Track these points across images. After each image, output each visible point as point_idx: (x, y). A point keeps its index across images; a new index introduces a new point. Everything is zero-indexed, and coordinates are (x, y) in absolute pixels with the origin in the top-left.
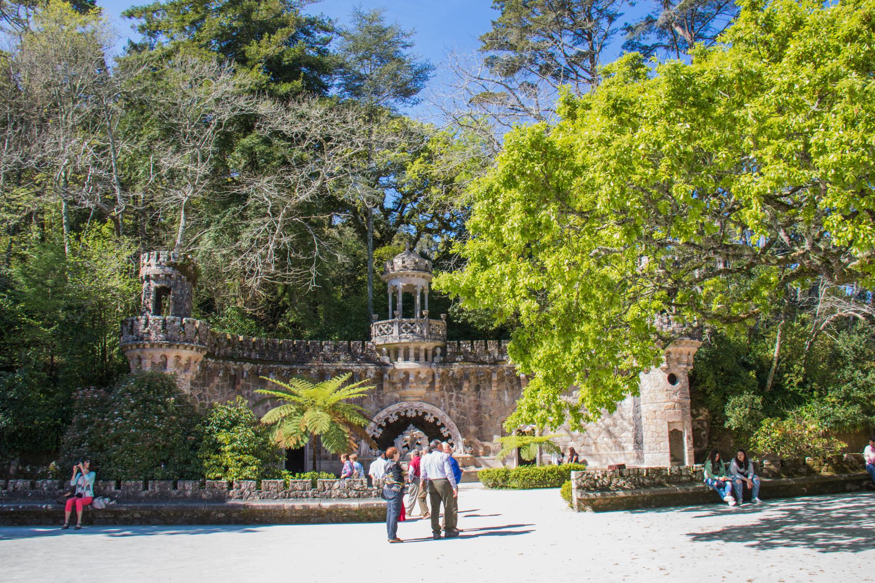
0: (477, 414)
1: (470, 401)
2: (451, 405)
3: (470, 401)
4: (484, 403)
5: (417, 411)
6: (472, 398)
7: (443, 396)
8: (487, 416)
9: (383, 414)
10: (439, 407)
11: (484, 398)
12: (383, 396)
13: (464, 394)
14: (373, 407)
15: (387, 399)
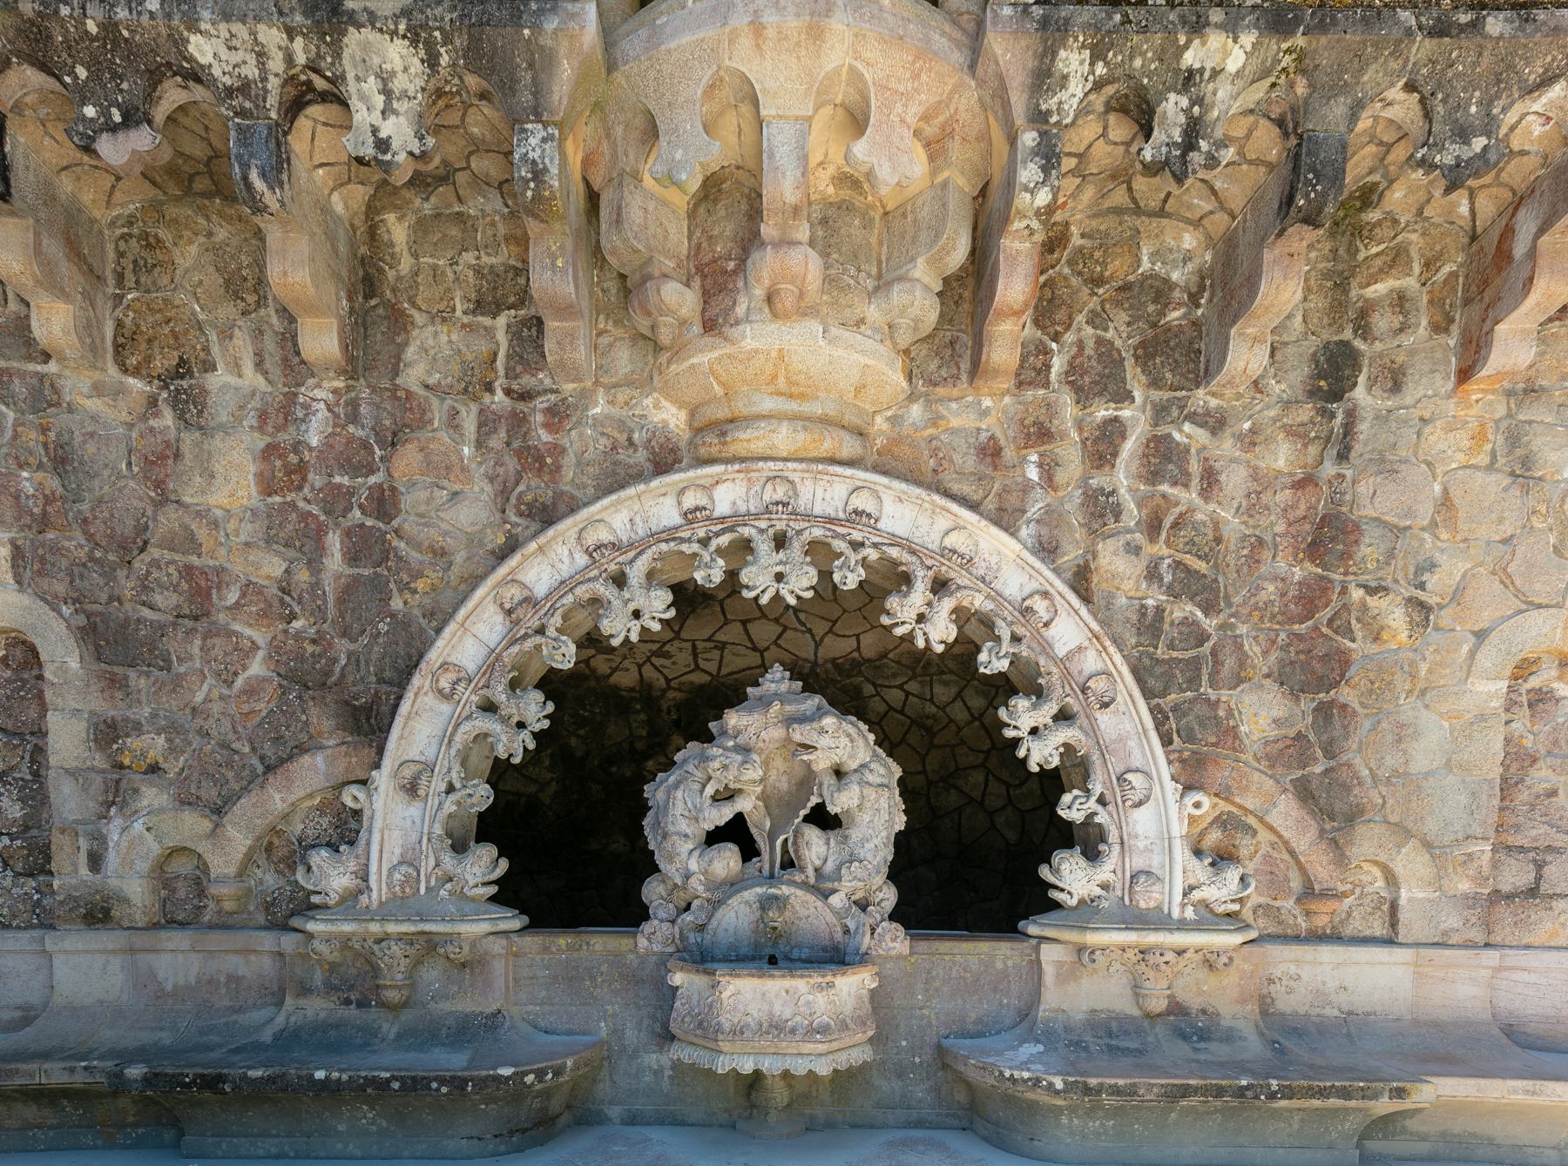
0: (1310, 598)
1: (1261, 481)
2: (1101, 508)
3: (1261, 481)
4: (1374, 499)
5: (819, 552)
6: (1282, 457)
7: (1040, 434)
8: (1396, 618)
9: (548, 564)
10: (1005, 519)
11: (1386, 467)
12: (557, 416)
13: (1215, 423)
14: (471, 513)
15: (582, 443)
